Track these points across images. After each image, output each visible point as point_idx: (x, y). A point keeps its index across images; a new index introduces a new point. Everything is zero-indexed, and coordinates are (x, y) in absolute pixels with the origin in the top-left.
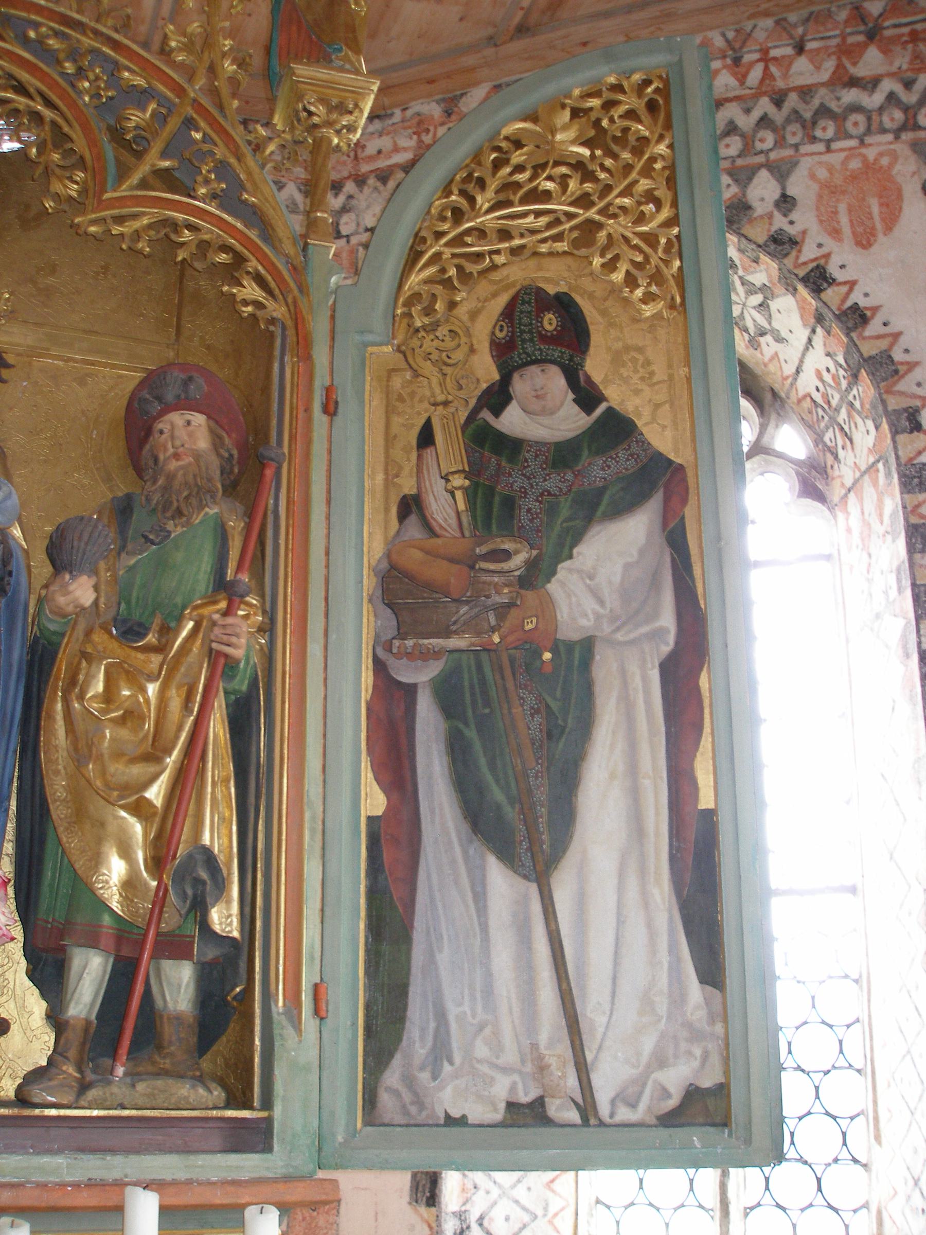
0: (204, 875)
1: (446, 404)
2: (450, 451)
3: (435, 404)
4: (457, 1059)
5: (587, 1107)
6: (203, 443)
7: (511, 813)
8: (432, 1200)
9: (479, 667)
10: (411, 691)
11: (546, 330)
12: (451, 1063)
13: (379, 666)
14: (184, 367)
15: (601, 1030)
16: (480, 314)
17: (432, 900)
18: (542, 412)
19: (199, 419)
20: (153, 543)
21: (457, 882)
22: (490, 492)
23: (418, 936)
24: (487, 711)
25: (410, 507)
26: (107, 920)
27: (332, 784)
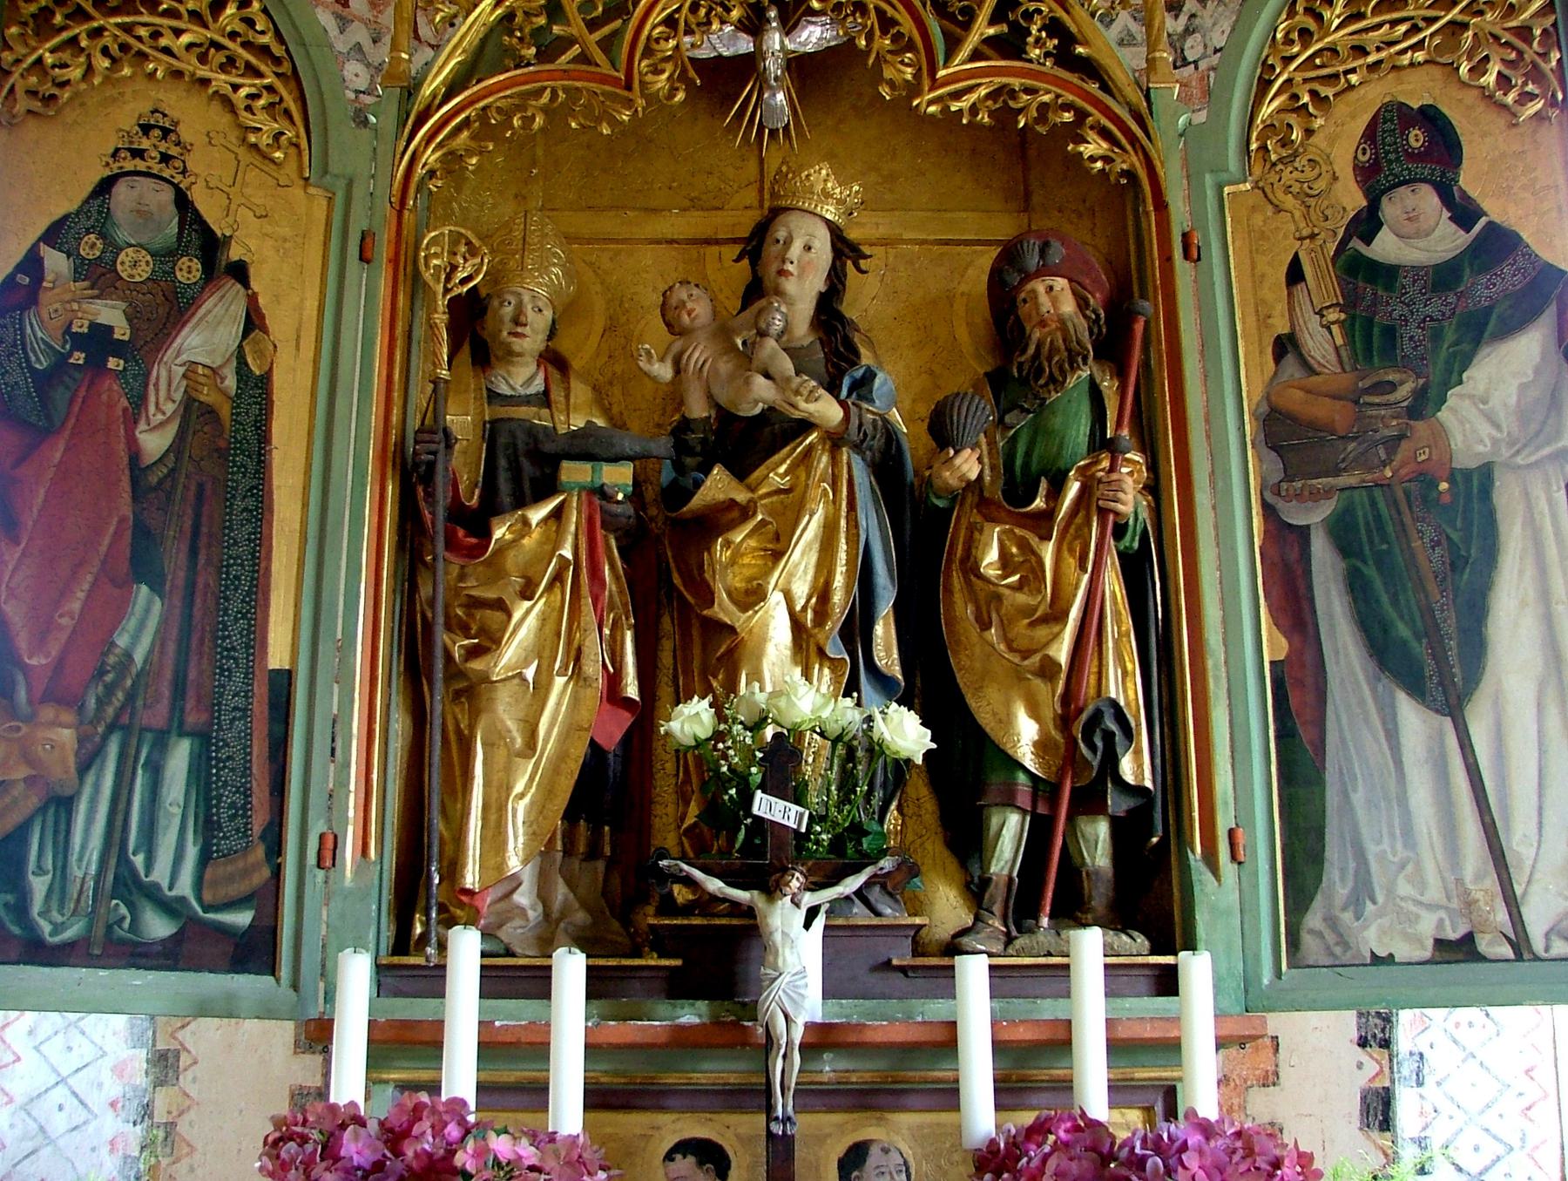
0: (1113, 727)
1: (1312, 236)
2: (1321, 284)
3: (1301, 239)
4: (1380, 899)
5: (1520, 944)
6: (1068, 306)
7: (1420, 649)
8: (1386, 1124)
9: (1373, 504)
10: (1304, 533)
12: (1374, 902)
13: (1268, 510)
14: (1039, 234)
15: (1529, 863)
16: (1340, 138)
17: (1343, 740)
18: (1418, 234)
19: (1060, 283)
20: (1028, 412)
21: (1367, 721)
22: (1369, 322)
23: (1331, 775)
24: (1384, 547)
25: (1285, 346)
26: (1022, 778)
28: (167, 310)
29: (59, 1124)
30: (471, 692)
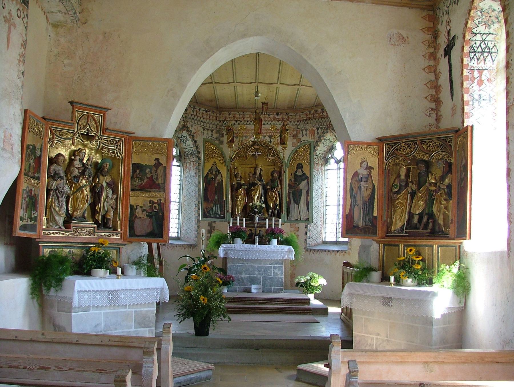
11: (300, 166)
16: (296, 166)
18: (299, 173)
25: (290, 180)
27: (285, 199)
28: (216, 176)
29: (189, 232)
30: (236, 201)
